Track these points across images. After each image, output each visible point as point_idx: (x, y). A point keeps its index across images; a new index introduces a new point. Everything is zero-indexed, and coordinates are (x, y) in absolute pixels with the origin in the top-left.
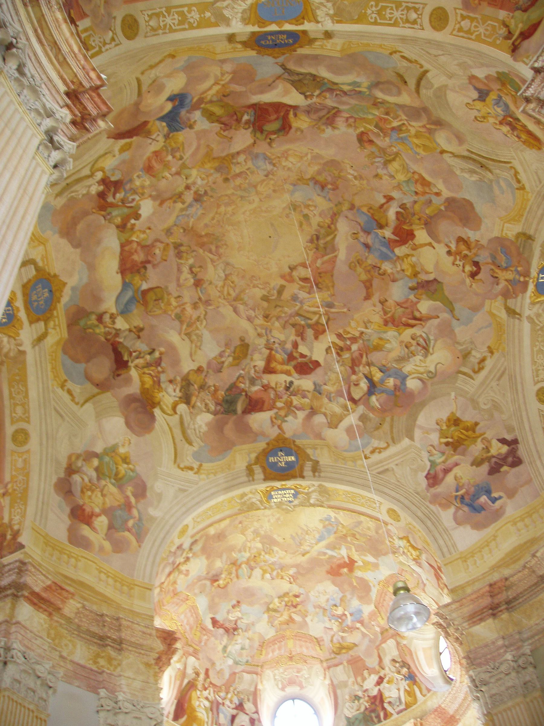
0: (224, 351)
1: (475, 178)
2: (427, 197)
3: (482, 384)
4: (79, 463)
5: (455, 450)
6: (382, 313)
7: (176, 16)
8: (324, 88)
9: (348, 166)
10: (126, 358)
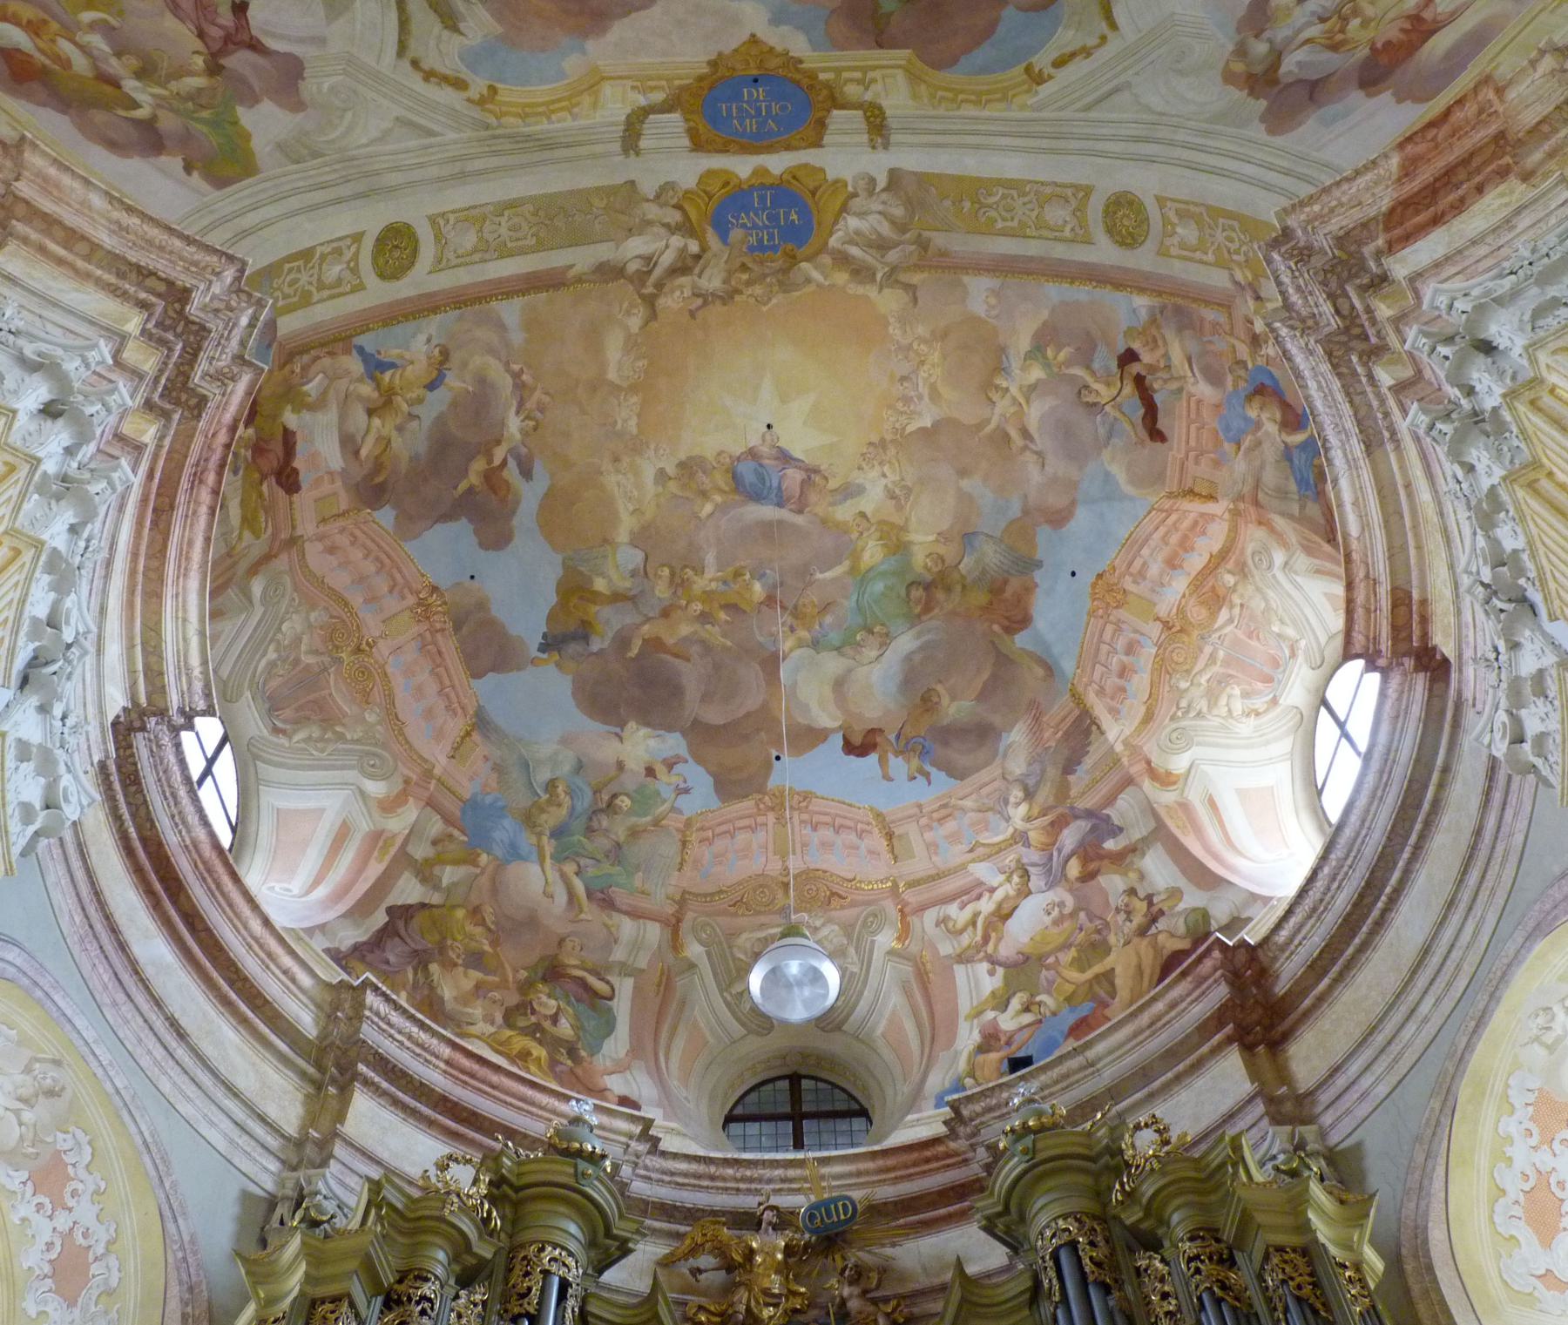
4: (1260, 48)
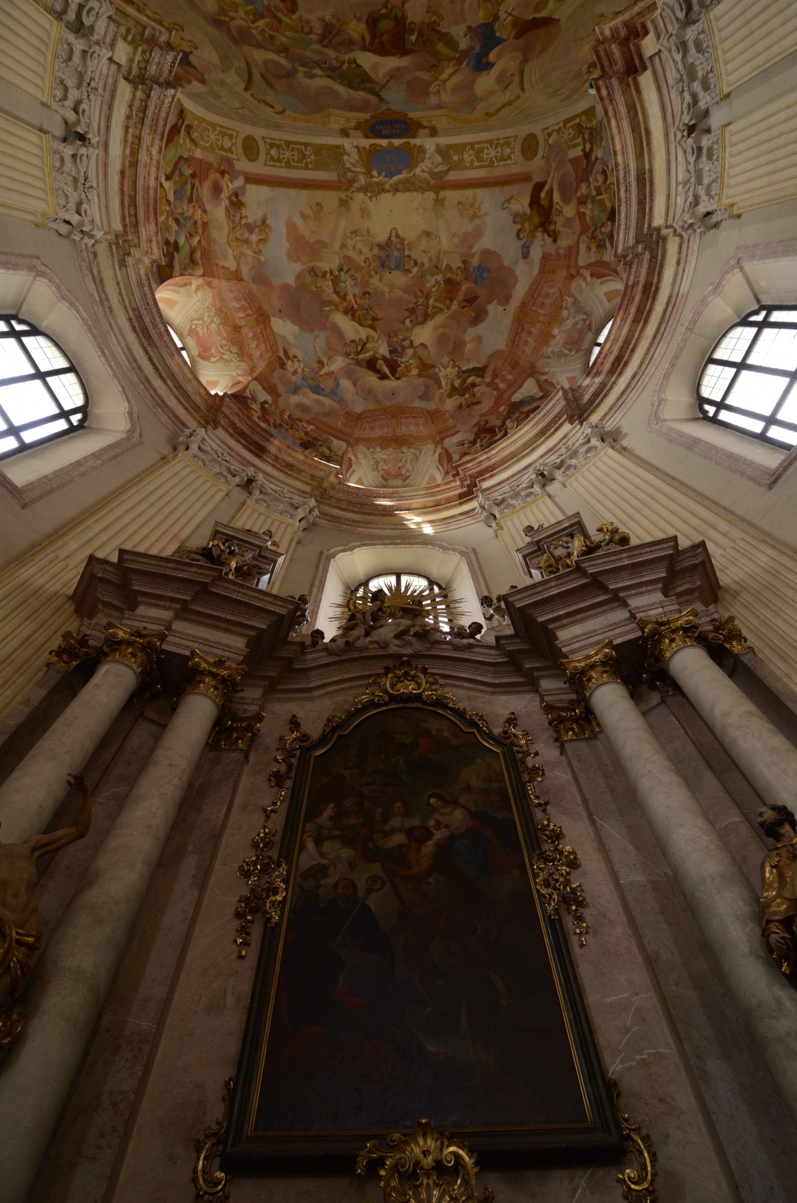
7: (485, 157)
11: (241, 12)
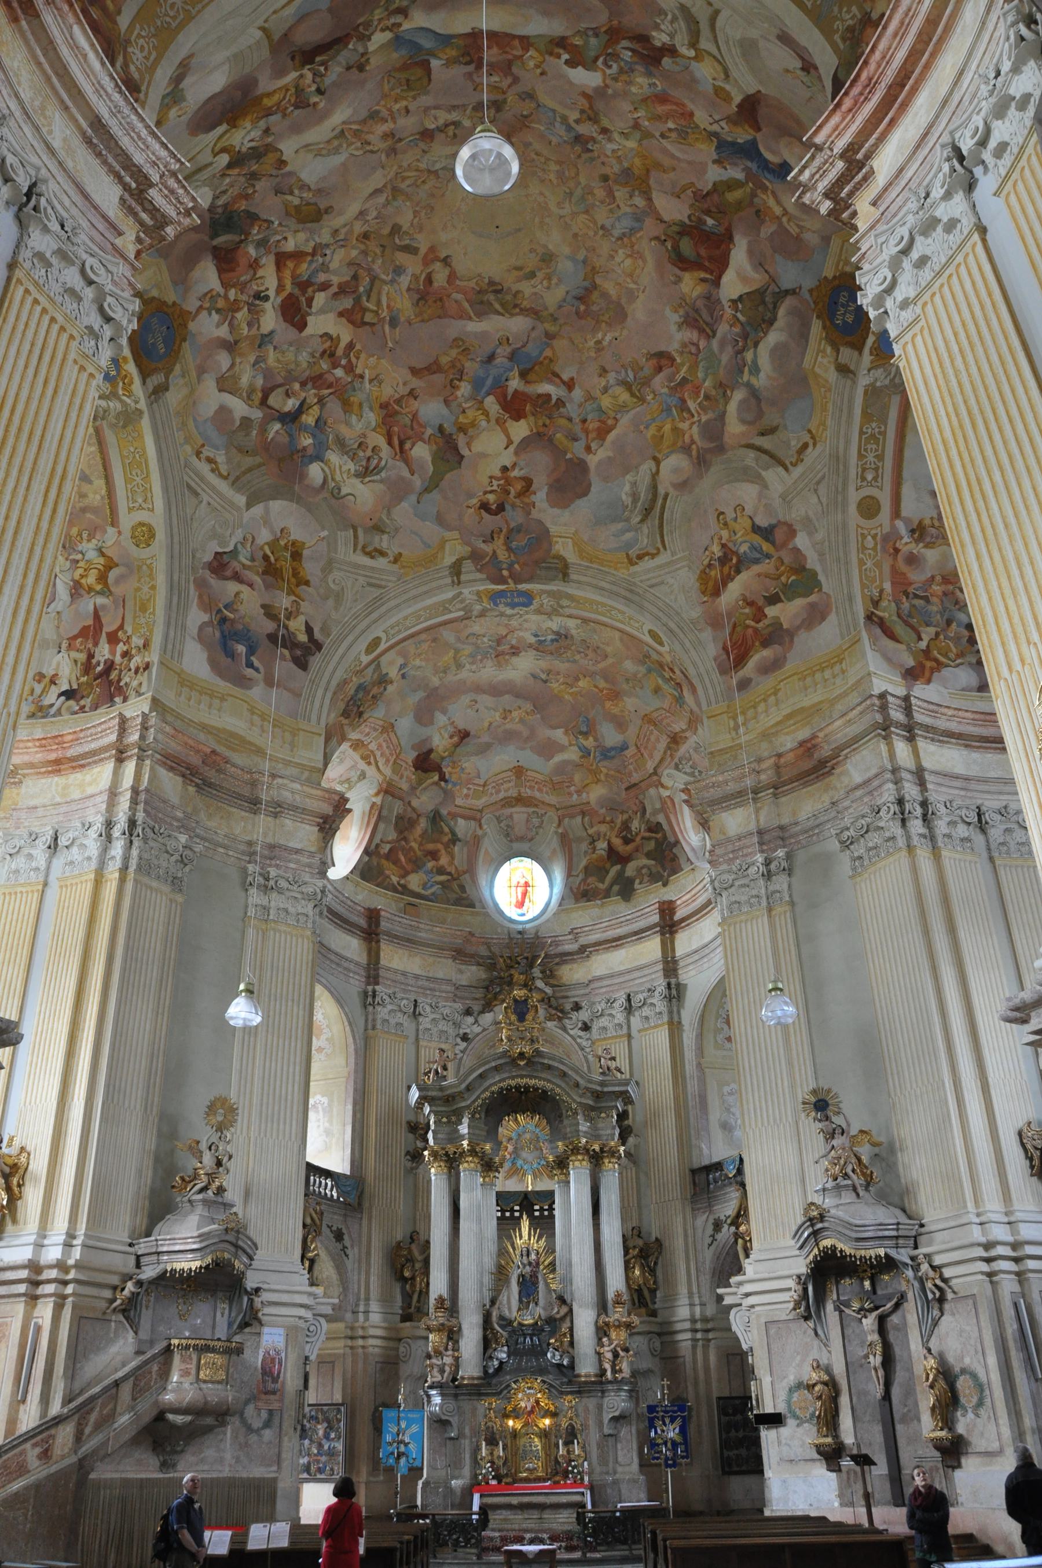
0: (309, 189)
1: (627, 500)
2: (583, 436)
3: (357, 566)
5: (264, 573)
6: (397, 396)
8: (748, 329)
9: (617, 334)
10: (318, 59)
11: (684, 426)
